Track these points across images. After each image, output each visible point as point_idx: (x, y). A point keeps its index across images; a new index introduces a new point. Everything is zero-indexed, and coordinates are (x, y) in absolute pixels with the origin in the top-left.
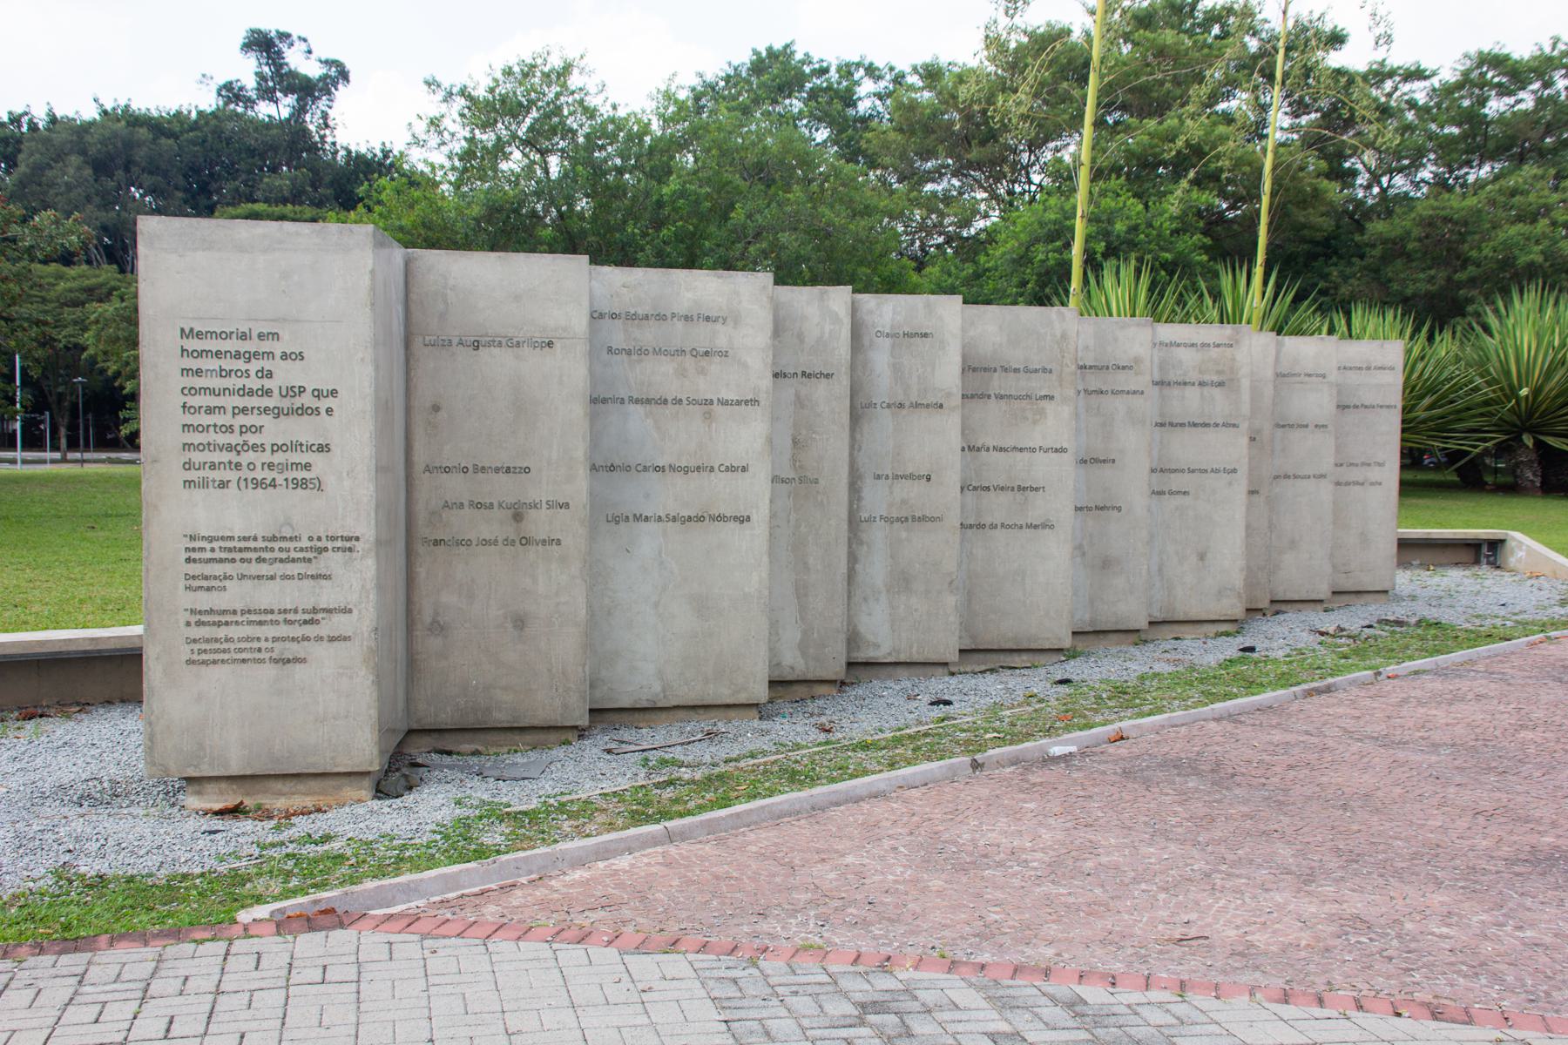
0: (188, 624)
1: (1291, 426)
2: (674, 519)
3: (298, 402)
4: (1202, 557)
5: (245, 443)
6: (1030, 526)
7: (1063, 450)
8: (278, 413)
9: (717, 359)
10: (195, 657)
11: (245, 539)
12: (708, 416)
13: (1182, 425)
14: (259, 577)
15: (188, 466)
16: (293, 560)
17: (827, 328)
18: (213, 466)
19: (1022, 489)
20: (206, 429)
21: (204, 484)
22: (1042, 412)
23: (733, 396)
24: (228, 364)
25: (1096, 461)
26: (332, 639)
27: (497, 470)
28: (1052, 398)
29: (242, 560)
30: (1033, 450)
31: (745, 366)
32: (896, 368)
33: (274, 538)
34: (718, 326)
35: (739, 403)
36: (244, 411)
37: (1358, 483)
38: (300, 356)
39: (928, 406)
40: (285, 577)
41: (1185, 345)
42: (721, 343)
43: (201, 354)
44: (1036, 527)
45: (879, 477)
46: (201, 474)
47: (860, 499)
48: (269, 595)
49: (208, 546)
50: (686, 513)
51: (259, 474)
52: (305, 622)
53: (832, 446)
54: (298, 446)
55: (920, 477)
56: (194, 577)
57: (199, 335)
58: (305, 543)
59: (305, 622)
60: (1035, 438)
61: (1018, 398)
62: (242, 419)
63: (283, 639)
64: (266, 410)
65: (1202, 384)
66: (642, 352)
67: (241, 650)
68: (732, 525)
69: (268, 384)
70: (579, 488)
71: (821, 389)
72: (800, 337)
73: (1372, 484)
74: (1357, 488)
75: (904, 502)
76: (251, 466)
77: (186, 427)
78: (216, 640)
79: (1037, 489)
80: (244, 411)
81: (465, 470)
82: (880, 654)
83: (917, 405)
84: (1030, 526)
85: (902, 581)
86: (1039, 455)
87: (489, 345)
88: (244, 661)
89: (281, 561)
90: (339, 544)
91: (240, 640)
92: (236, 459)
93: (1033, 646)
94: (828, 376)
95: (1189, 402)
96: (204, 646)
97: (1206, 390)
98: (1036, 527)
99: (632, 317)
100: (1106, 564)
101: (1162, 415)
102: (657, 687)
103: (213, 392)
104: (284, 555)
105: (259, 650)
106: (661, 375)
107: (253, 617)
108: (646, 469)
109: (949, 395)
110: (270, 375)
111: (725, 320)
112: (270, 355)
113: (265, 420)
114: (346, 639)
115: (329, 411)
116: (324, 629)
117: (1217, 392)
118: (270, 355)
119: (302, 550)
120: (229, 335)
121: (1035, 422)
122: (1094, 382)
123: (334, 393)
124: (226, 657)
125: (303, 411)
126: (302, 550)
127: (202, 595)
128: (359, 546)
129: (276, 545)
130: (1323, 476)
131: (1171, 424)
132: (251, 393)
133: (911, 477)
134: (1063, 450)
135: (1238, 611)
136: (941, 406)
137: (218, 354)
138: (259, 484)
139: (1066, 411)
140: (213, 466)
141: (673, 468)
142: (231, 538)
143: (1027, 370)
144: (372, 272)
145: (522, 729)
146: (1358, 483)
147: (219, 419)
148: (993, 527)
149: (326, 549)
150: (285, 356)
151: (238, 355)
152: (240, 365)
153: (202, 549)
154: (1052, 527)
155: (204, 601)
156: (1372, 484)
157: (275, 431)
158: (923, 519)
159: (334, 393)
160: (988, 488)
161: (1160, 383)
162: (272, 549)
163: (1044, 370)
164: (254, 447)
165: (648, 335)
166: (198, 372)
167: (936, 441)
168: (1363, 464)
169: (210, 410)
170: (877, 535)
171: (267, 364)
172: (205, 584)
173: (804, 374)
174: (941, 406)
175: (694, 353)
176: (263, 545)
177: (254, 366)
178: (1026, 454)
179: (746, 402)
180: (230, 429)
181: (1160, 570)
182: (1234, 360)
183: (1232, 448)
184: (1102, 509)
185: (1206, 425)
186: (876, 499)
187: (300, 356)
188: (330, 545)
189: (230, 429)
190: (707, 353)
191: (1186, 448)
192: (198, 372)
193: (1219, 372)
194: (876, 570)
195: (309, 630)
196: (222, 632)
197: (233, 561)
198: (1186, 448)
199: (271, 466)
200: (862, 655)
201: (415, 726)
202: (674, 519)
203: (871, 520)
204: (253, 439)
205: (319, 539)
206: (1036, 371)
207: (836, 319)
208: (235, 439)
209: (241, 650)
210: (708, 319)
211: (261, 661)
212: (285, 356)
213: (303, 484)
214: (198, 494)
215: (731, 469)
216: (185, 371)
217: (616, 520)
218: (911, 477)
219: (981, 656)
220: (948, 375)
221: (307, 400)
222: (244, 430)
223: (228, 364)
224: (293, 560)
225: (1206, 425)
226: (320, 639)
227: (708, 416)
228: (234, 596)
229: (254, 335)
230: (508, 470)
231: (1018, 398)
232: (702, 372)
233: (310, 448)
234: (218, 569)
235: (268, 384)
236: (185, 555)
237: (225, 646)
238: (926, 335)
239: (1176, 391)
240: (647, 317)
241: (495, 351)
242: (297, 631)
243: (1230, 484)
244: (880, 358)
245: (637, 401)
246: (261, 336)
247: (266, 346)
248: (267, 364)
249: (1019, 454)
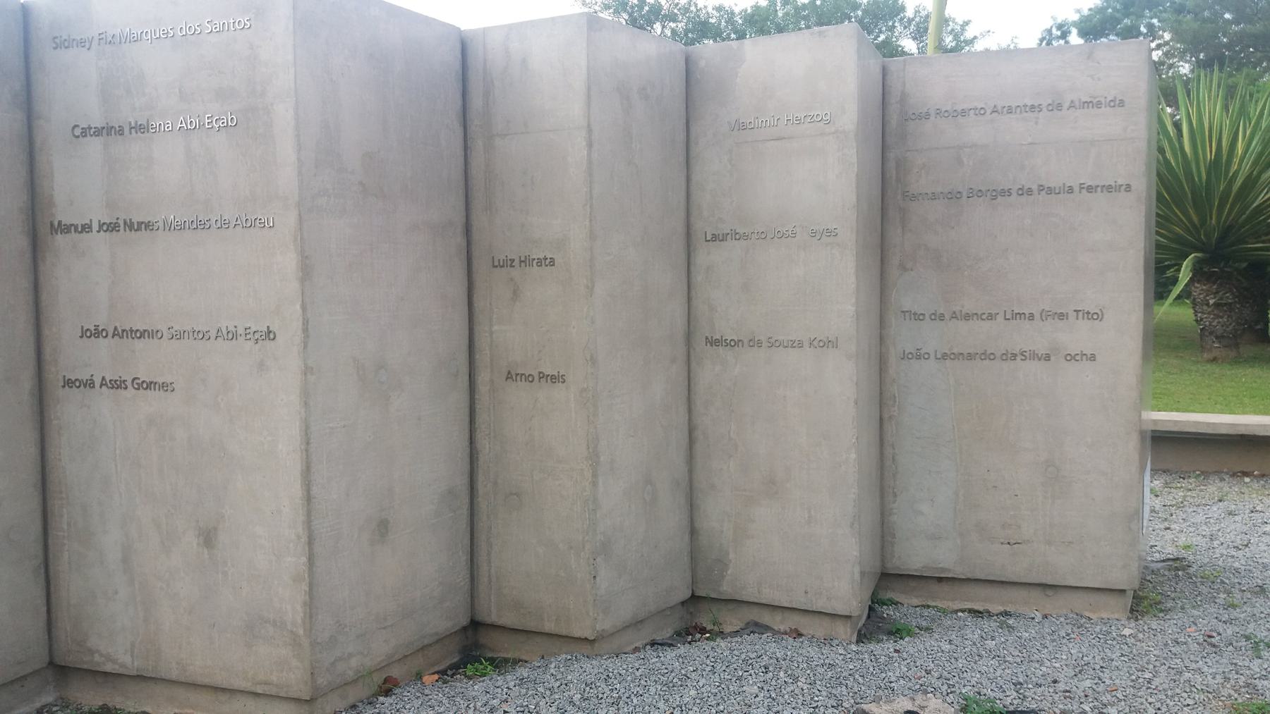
1: (763, 236)
4: (208, 538)
37: (1034, 356)
73: (1071, 358)
74: (1033, 366)
130: (829, 343)
146: (1034, 356)
156: (1071, 358)
168: (1045, 315)
181: (126, 560)
185: (201, 225)
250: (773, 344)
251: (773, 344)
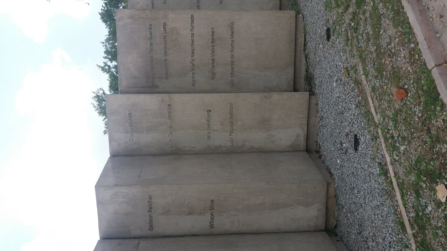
6: (232, 36)
7: (192, 17)
19: (213, 41)
28: (165, 24)
30: (193, 35)
44: (233, 33)
45: (209, 137)
61: (165, 42)
79: (213, 32)
82: (302, 133)
83: (170, 117)
84: (232, 36)
85: (264, 124)
86: (195, 31)
93: (294, 33)
94: (150, 198)
98: (233, 33)
133: (209, 121)
134: (192, 17)
136: (169, 105)
139: (171, 16)
148: (232, 56)
154: (233, 23)
158: (231, 114)
160: (213, 60)
163: (150, 28)
173: (149, 211)
174: (169, 105)
178: (195, 38)
186: (221, 139)
194: (258, 138)
206: (151, 33)
218: (209, 121)
249: (195, 43)
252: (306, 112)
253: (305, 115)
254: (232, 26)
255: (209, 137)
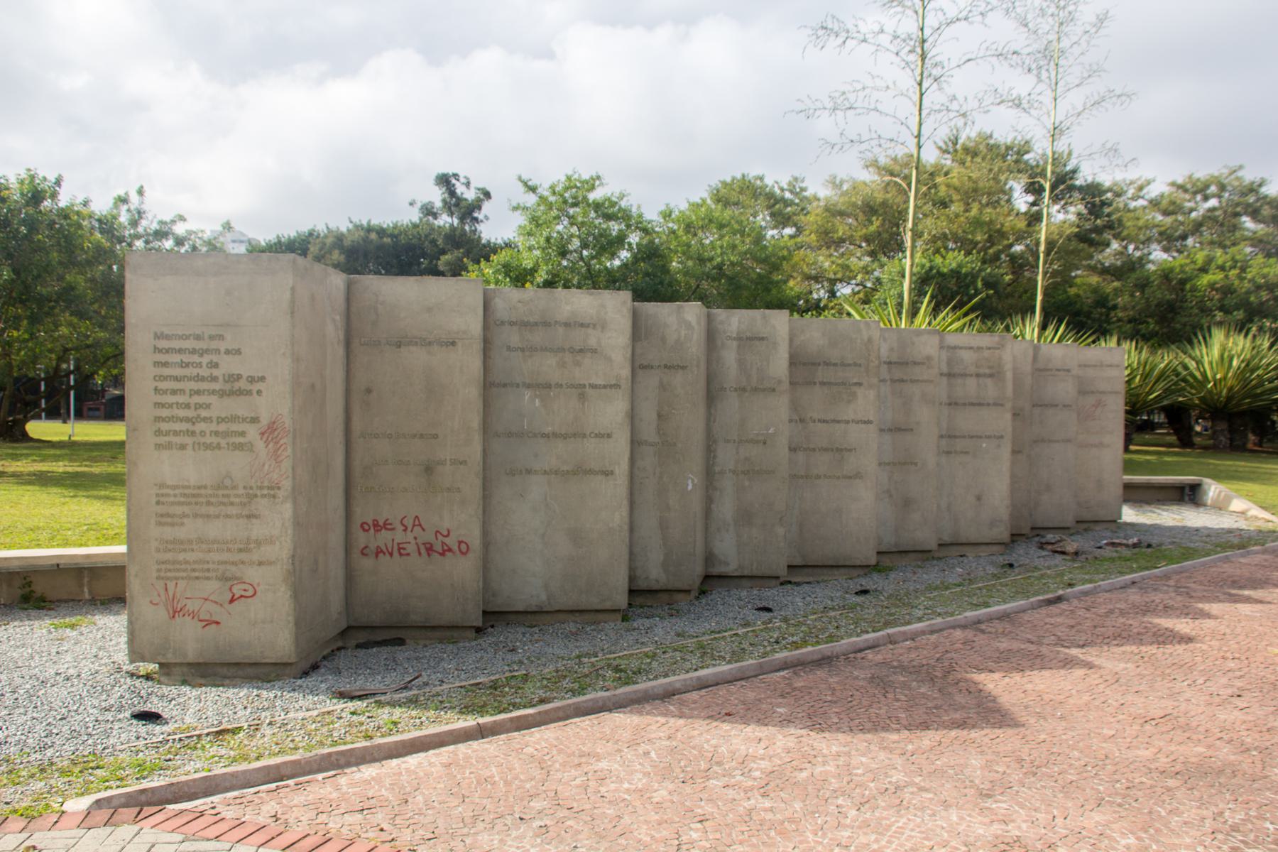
0: (158, 550)
2: (556, 473)
3: (237, 385)
5: (199, 416)
7: (869, 422)
8: (222, 394)
9: (589, 355)
10: (162, 574)
11: (199, 488)
12: (582, 397)
13: (964, 404)
14: (208, 516)
15: (158, 433)
16: (232, 504)
17: (683, 333)
18: (176, 433)
20: (171, 406)
21: (169, 446)
22: (854, 395)
23: (600, 382)
24: (186, 358)
25: (900, 429)
26: (260, 564)
27: (415, 436)
28: (860, 384)
29: (196, 503)
30: (847, 422)
31: (609, 359)
32: (741, 363)
33: (219, 487)
34: (590, 331)
35: (605, 387)
36: (198, 392)
38: (238, 352)
39: (764, 390)
40: (227, 516)
41: (966, 348)
42: (592, 342)
43: (167, 351)
44: (850, 477)
45: (728, 441)
46: (167, 439)
47: (715, 457)
48: (214, 530)
49: (172, 492)
50: (565, 468)
51: (208, 439)
52: (240, 550)
53: (690, 420)
54: (234, 419)
55: (757, 442)
56: (162, 516)
57: (168, 337)
58: (241, 491)
59: (240, 550)
60: (849, 413)
61: (836, 384)
62: (197, 399)
63: (226, 563)
64: (213, 392)
65: (978, 375)
66: (533, 349)
67: (194, 570)
68: (600, 477)
69: (215, 372)
70: (475, 450)
71: (678, 379)
72: (663, 339)
75: (746, 459)
76: (203, 433)
77: (158, 405)
78: (179, 563)
79: (850, 450)
80: (198, 392)
81: (390, 436)
82: (731, 568)
83: (756, 390)
85: (745, 517)
86: (853, 427)
87: (410, 343)
88: (197, 578)
89: (224, 504)
90: (265, 492)
91: (195, 562)
92: (191, 428)
94: (684, 368)
95: (969, 388)
96: (169, 567)
97: (981, 380)
98: (850, 477)
99: (524, 325)
100: (907, 503)
101: (949, 397)
102: (544, 597)
103: (177, 379)
104: (225, 500)
105: (208, 570)
106: (547, 366)
107: (204, 546)
108: (535, 436)
109: (780, 382)
110: (216, 365)
111: (594, 326)
112: (218, 351)
113: (213, 399)
114: (270, 563)
115: (259, 392)
116: (255, 557)
117: (989, 382)
118: (218, 351)
119: (237, 496)
120: (187, 337)
121: (849, 402)
122: (898, 374)
123: (262, 379)
124: (184, 574)
125: (240, 392)
126: (237, 496)
127: (168, 530)
128: (281, 494)
129: (221, 492)
130: (1069, 441)
131: (956, 404)
132: (203, 379)
134: (869, 422)
135: (1005, 536)
136: (774, 390)
137: (180, 351)
138: (208, 447)
139: (872, 394)
140: (176, 433)
141: (555, 435)
142: (189, 487)
143: (843, 365)
144: (293, 289)
145: (433, 628)
147: (181, 399)
148: (818, 477)
149: (256, 496)
150: (228, 352)
151: (193, 351)
152: (196, 358)
153: (168, 495)
154: (861, 478)
155: (169, 533)
157: (220, 407)
159: (262, 379)
160: (814, 450)
161: (950, 375)
162: (217, 496)
163: (855, 364)
164: (205, 419)
165: (538, 337)
166: (165, 364)
167: (773, 415)
169: (174, 392)
170: (727, 484)
171: (215, 358)
172: (169, 520)
173: (666, 366)
175: (572, 350)
176: (210, 492)
177: (205, 360)
178: (843, 426)
179: (611, 386)
180: (187, 406)
182: (1000, 358)
183: (1002, 421)
184: (905, 463)
186: (726, 457)
187: (238, 352)
188: (259, 493)
189: (187, 406)
190: (581, 351)
191: (967, 421)
192: (165, 364)
193: (990, 367)
194: (726, 508)
195: (243, 556)
196: (181, 557)
197: (190, 504)
198: (967, 421)
199: (217, 433)
200: (715, 571)
201: (353, 624)
202: (556, 473)
203: (722, 472)
204: (204, 413)
205: (251, 488)
206: (849, 365)
207: (689, 326)
208: (190, 413)
209: (194, 570)
210: (582, 325)
211: (208, 578)
212: (228, 352)
213: (240, 447)
214: (165, 454)
215: (599, 436)
216: (157, 364)
217: (512, 473)
219: (810, 570)
220: (779, 365)
221: (242, 384)
222: (199, 406)
223: (186, 358)
224: (232, 504)
225: (980, 404)
226: (251, 563)
227: (582, 397)
228: (190, 529)
229: (206, 336)
230: (422, 436)
231: (836, 384)
232: (578, 364)
233: (244, 420)
234: (178, 510)
235: (215, 372)
236: (154, 500)
237: (183, 567)
238: (763, 339)
239: (959, 381)
240: (536, 324)
241: (413, 349)
242: (237, 557)
243: (999, 446)
244: (730, 356)
245: (529, 386)
246: (212, 338)
247: (214, 344)
248: (215, 358)
250: (1050, 441)
251: (1050, 441)
252: (760, 574)
253: (755, 573)
254: (858, 476)
255: (728, 441)
